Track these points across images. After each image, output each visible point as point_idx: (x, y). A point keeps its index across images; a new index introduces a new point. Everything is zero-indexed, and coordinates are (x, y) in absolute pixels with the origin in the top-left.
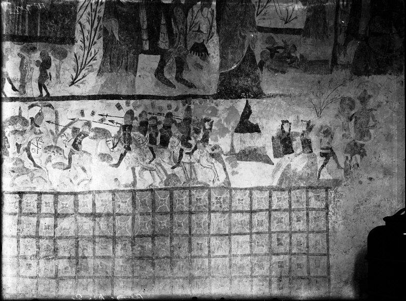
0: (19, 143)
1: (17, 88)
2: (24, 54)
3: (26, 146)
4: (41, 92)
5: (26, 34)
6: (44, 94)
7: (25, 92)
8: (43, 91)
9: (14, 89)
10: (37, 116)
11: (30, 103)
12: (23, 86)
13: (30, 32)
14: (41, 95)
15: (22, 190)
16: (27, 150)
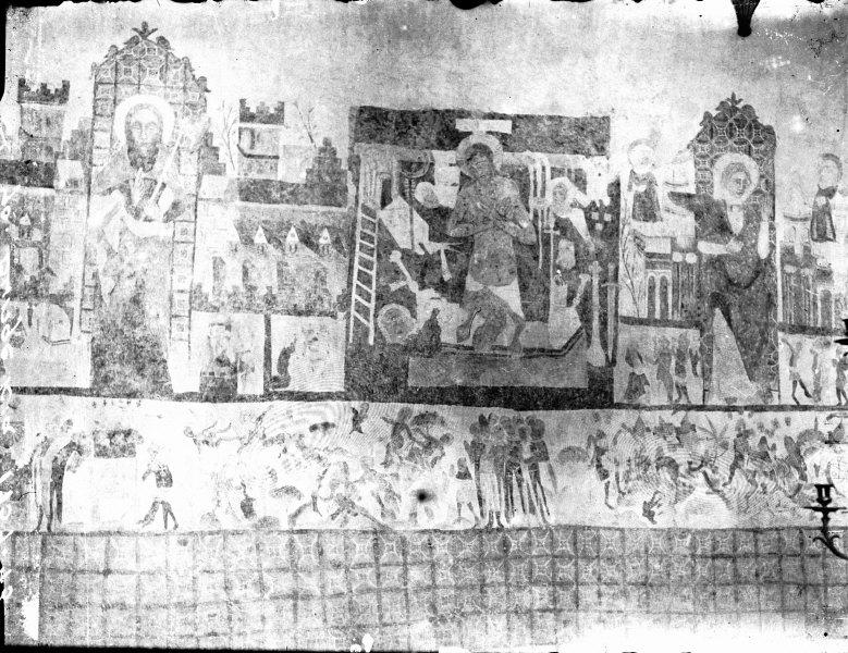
2: (818, 351)
3: (825, 468)
4: (840, 399)
5: (819, 326)
6: (844, 402)
7: (820, 399)
8: (842, 397)
9: (807, 394)
10: (835, 431)
11: (829, 413)
12: (818, 391)
13: (823, 323)
14: (840, 404)
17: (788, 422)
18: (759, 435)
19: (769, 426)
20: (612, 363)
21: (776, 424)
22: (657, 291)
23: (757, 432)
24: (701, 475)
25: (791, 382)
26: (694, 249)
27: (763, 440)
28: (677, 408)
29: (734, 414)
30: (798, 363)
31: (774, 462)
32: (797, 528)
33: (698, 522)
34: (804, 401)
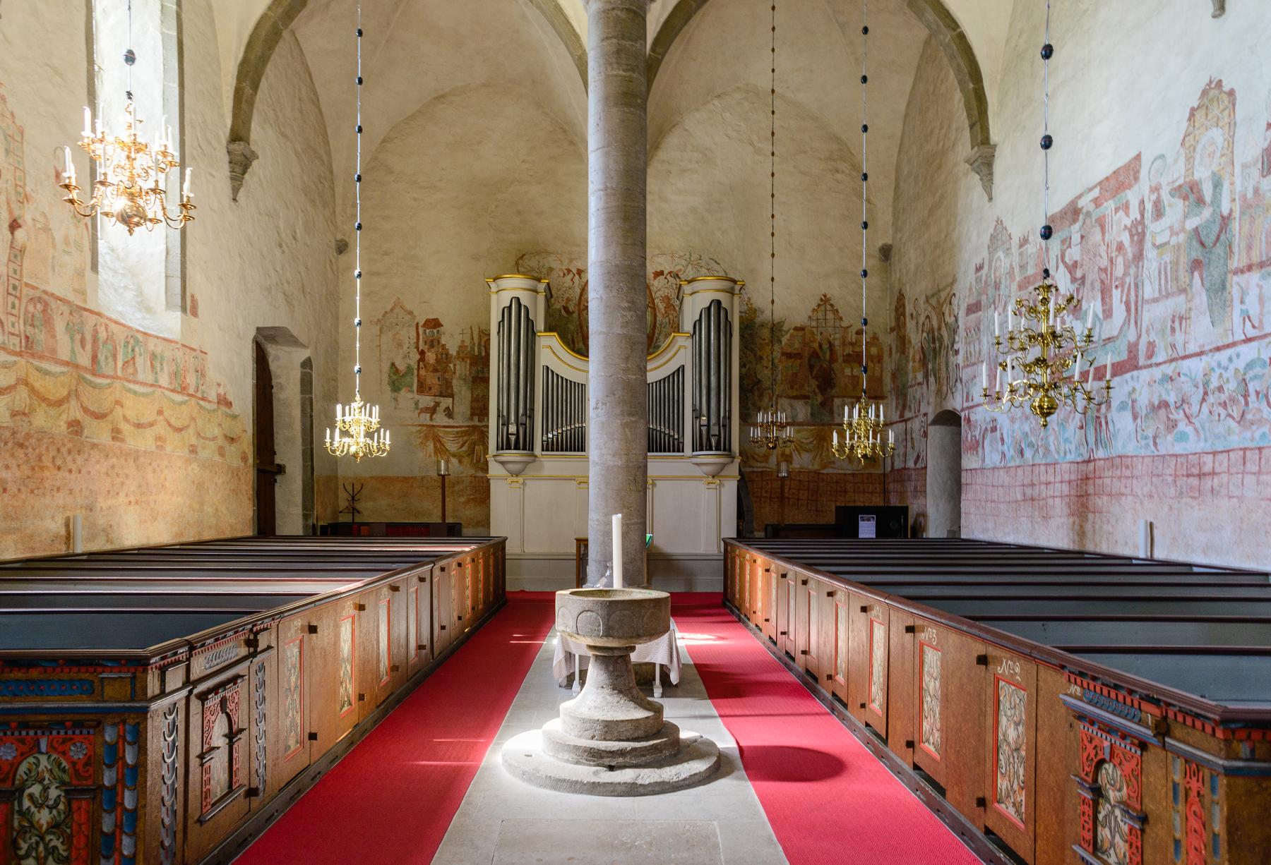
0: (1258, 389)
1: (1256, 325)
2: (1262, 283)
9: (1254, 327)
15: (1262, 444)
16: (1267, 397)
17: (1238, 356)
18: (1218, 371)
19: (1225, 362)
20: (1139, 337)
21: (1230, 359)
22: (1163, 273)
23: (1216, 369)
24: (1181, 412)
25: (1242, 318)
26: (1183, 229)
27: (1221, 375)
28: (1172, 360)
29: (1204, 357)
30: (1247, 299)
31: (1227, 394)
32: (1241, 449)
33: (1179, 449)
34: (1251, 333)
